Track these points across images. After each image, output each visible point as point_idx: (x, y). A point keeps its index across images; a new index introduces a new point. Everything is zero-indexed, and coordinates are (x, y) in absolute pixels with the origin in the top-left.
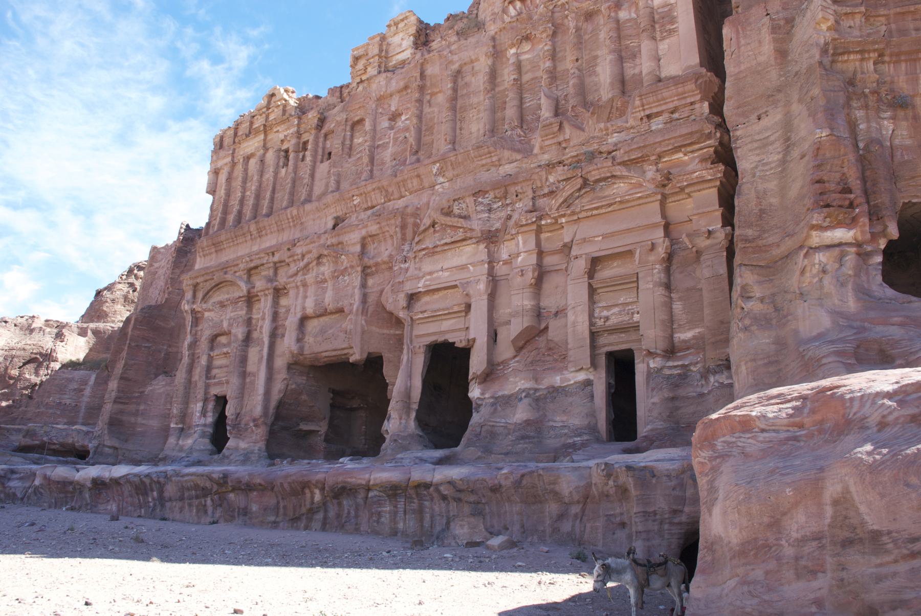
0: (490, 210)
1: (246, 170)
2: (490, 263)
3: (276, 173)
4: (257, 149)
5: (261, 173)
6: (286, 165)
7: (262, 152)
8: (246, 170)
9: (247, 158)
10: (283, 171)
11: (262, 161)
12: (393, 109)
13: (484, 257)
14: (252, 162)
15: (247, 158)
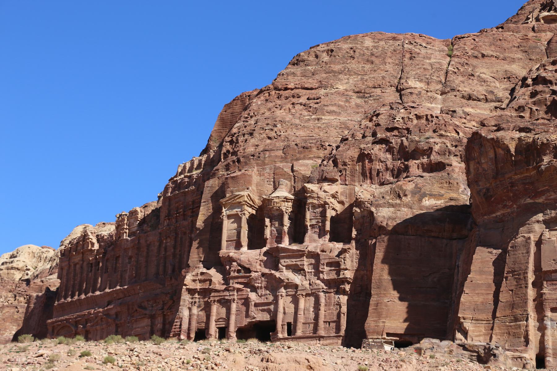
0: (152, 307)
1: (75, 270)
2: (151, 326)
3: (87, 275)
4: (79, 261)
5: (82, 273)
6: (91, 271)
7: (81, 262)
8: (75, 270)
9: (75, 265)
10: (90, 274)
11: (82, 267)
12: (130, 254)
13: (150, 324)
14: (78, 266)
15: (75, 265)
